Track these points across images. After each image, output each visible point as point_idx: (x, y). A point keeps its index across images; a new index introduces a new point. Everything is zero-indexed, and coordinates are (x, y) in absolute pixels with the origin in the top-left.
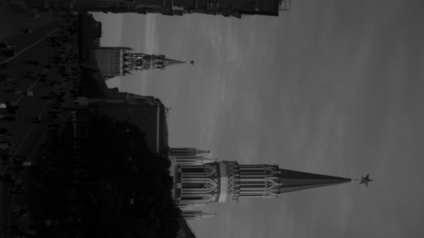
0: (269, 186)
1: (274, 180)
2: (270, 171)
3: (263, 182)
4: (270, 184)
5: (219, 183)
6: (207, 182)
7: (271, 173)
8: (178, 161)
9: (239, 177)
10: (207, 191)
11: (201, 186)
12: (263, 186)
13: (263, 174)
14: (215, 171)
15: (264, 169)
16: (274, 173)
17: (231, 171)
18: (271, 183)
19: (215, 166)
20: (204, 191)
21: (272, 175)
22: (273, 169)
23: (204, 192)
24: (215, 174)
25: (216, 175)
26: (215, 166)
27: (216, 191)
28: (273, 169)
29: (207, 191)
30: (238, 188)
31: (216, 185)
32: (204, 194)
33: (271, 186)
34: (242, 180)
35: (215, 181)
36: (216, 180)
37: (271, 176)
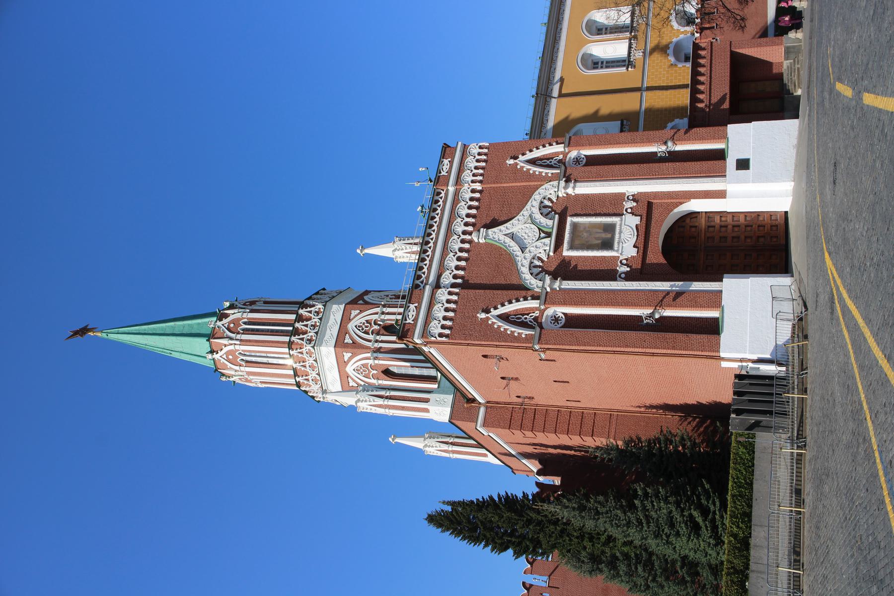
0: (236, 322)
3: (246, 331)
4: (232, 325)
5: (343, 330)
6: (371, 337)
7: (228, 353)
10: (377, 313)
14: (349, 369)
16: (220, 353)
18: (229, 329)
19: (352, 383)
20: (383, 313)
21: (225, 350)
22: (226, 368)
23: (384, 309)
24: (350, 359)
26: (352, 383)
27: (354, 313)
28: (226, 368)
29: (377, 313)
30: (300, 319)
31: (351, 326)
32: (384, 306)
33: (229, 323)
34: (287, 339)
35: (351, 338)
36: (348, 340)
37: (225, 346)
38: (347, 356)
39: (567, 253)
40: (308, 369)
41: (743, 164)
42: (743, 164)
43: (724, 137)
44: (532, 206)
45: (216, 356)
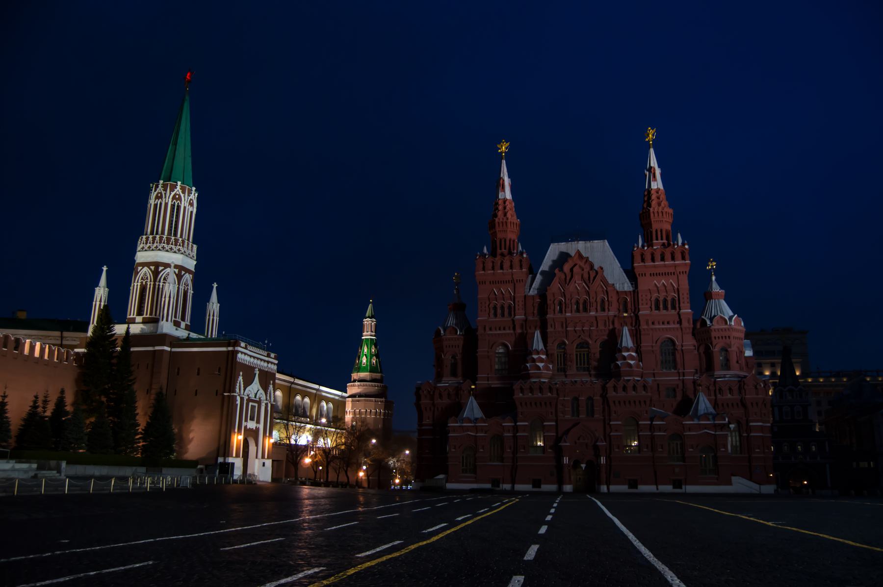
1: (189, 196)
2: (176, 194)
5: (187, 271)
7: (179, 195)
8: (167, 320)
9: (183, 242)
11: (185, 293)
12: (192, 212)
13: (179, 207)
15: (170, 200)
17: (171, 249)
21: (182, 195)
22: (172, 190)
25: (177, 271)
26: (161, 268)
38: (177, 271)
39: (251, 404)
40: (170, 246)
41: (264, 465)
42: (264, 465)
43: (268, 458)
44: (261, 391)
45: (179, 187)
